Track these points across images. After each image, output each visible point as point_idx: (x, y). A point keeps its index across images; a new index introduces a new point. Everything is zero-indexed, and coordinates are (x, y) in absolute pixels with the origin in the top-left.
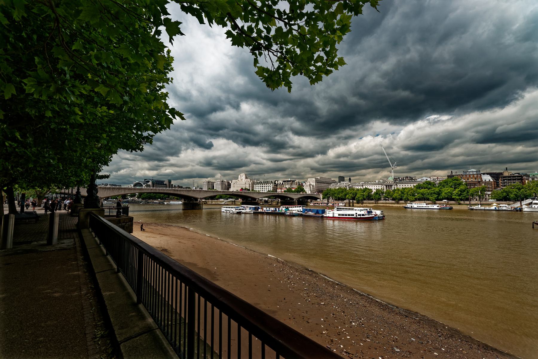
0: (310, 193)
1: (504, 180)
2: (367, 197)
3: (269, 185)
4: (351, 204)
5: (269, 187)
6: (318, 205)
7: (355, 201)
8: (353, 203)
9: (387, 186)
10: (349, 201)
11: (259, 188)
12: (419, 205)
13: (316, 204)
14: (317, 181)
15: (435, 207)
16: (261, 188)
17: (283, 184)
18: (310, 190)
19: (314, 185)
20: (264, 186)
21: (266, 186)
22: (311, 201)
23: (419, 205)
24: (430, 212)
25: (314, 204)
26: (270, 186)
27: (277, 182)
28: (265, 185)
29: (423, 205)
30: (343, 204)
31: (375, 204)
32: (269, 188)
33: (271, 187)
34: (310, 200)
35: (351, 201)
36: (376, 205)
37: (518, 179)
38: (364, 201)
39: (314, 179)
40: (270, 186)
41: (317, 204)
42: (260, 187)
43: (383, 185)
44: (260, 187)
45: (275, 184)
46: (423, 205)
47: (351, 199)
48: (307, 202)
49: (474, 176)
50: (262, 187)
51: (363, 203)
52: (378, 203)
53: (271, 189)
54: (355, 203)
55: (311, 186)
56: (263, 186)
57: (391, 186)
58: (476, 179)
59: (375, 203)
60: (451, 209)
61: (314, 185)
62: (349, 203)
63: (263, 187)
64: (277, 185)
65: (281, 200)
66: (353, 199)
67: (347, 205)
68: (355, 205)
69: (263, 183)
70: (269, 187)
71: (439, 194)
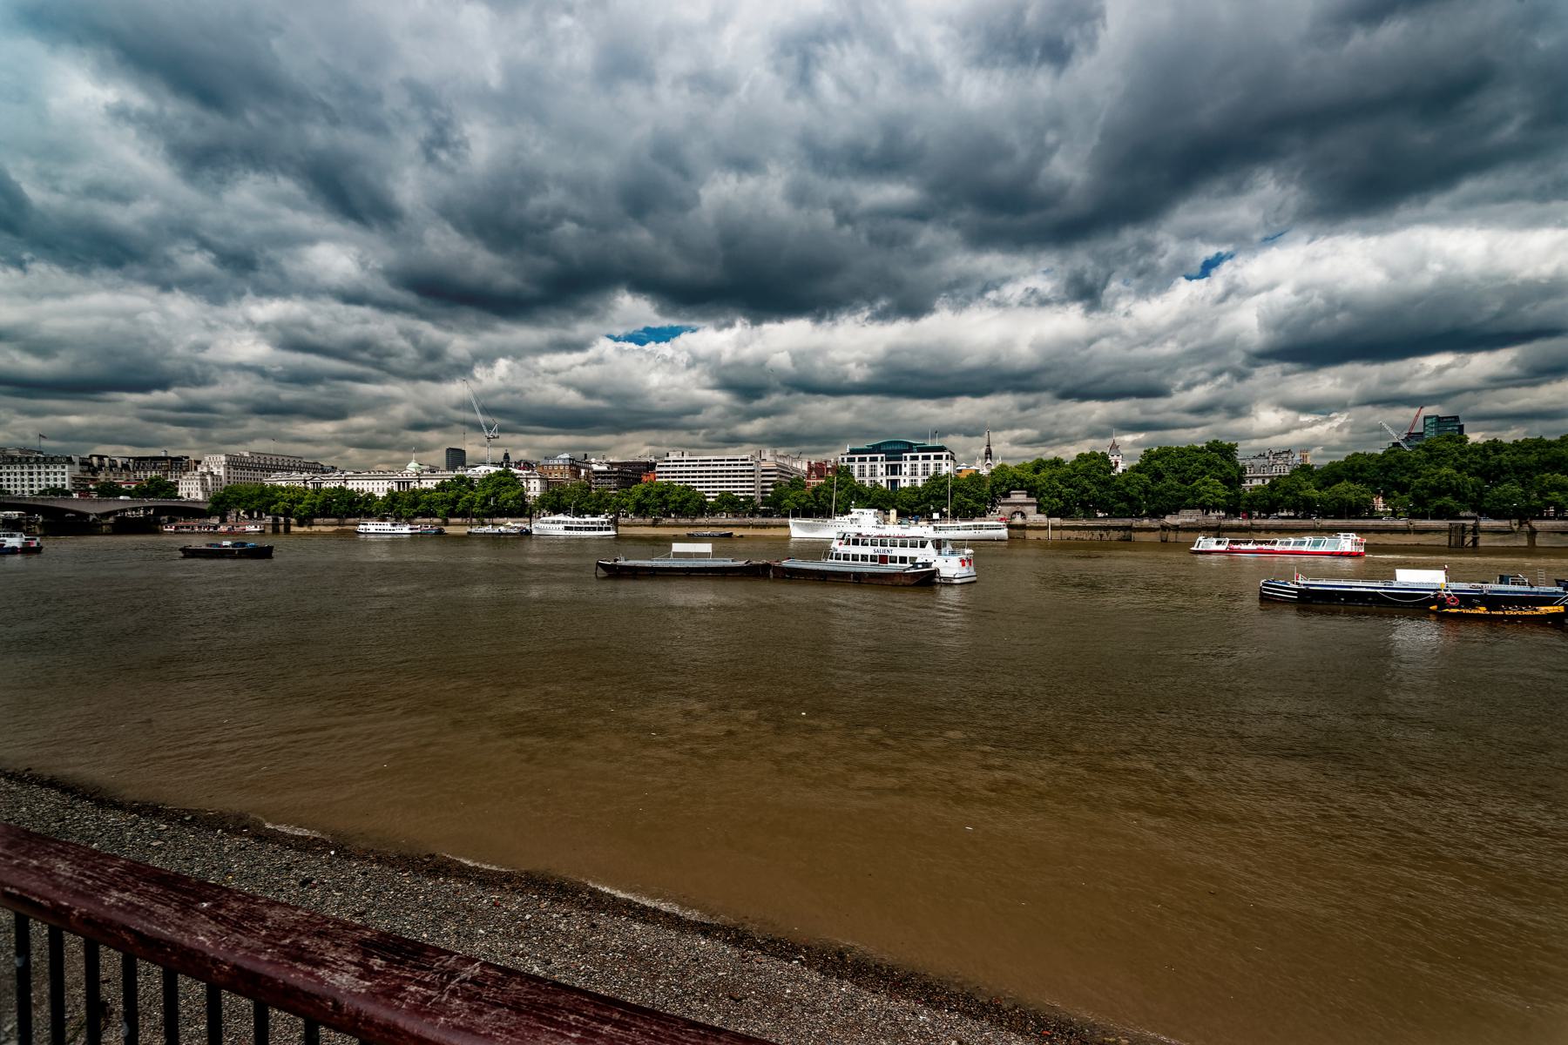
0: (200, 497)
1: (596, 478)
2: (320, 509)
3: (59, 469)
4: (282, 528)
5: (59, 476)
6: (189, 530)
7: (293, 520)
8: (287, 525)
9: (399, 483)
10: (276, 520)
11: (18, 477)
12: (379, 527)
13: (182, 527)
14: (234, 463)
15: (406, 529)
16: (18, 477)
17: (125, 467)
18: (205, 490)
19: (222, 474)
20: (39, 473)
21: (47, 474)
22: (171, 521)
23: (379, 527)
24: (395, 542)
25: (176, 528)
26: (63, 474)
27: (95, 460)
28: (42, 470)
29: (387, 526)
30: (256, 527)
31: (337, 527)
32: (56, 480)
33: (66, 476)
34: (166, 518)
35: (282, 519)
36: (340, 528)
37: (615, 478)
38: (316, 520)
39: (223, 458)
40: (63, 474)
41: (188, 527)
42: (22, 474)
43: (393, 481)
44: (22, 474)
45: (86, 468)
46: (385, 527)
47: (282, 516)
48: (159, 523)
49: (559, 469)
50: (31, 474)
51: (311, 525)
52: (344, 525)
53: (66, 483)
54: (295, 525)
55: (209, 478)
56: (35, 470)
57: (408, 483)
58: (562, 473)
59: (339, 525)
60: (440, 533)
61: (222, 474)
62: (275, 525)
63: (35, 477)
64: (94, 471)
65: (44, 517)
66: (288, 513)
67: (269, 530)
68: (293, 529)
69: (32, 461)
70: (59, 476)
71: (455, 502)
